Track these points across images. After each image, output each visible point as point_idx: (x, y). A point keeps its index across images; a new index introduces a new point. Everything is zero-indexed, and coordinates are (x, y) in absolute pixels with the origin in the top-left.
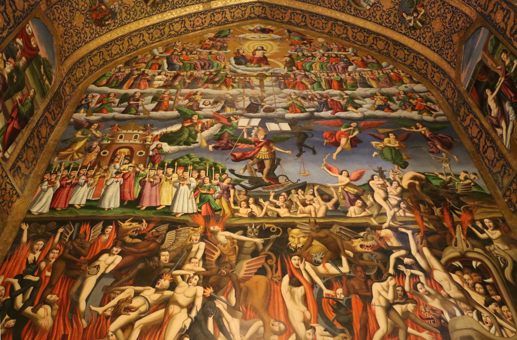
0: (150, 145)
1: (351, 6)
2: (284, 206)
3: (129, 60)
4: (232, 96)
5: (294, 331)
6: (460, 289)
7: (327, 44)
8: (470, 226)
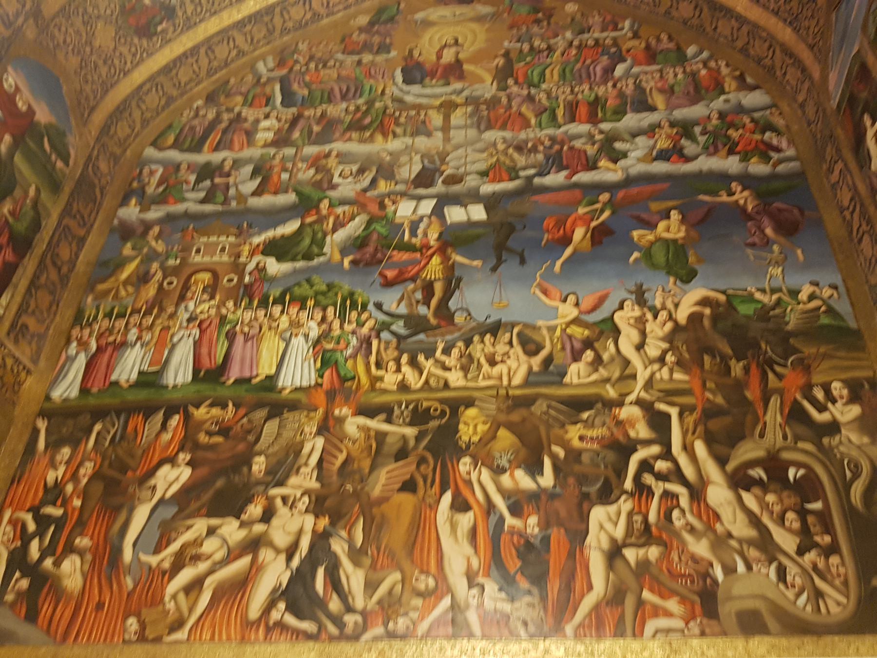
0: (245, 265)
3: (214, 91)
4: (391, 154)
5: (449, 590)
6: (754, 520)
7: (582, 15)
8: (799, 397)
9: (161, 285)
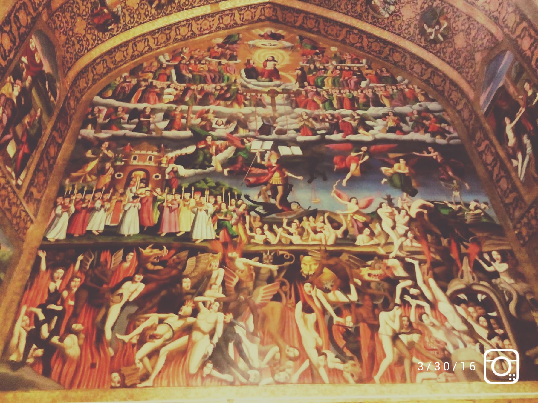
0: (166, 168)
1: (368, 13)
2: (297, 233)
3: (135, 68)
5: (308, 357)
7: (340, 53)
8: (477, 258)
9: (113, 176)
